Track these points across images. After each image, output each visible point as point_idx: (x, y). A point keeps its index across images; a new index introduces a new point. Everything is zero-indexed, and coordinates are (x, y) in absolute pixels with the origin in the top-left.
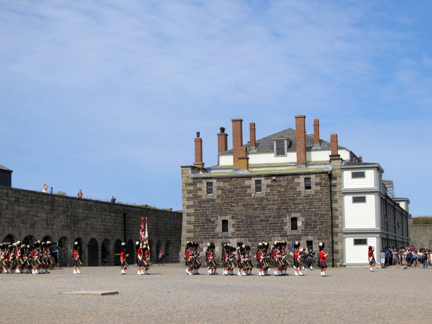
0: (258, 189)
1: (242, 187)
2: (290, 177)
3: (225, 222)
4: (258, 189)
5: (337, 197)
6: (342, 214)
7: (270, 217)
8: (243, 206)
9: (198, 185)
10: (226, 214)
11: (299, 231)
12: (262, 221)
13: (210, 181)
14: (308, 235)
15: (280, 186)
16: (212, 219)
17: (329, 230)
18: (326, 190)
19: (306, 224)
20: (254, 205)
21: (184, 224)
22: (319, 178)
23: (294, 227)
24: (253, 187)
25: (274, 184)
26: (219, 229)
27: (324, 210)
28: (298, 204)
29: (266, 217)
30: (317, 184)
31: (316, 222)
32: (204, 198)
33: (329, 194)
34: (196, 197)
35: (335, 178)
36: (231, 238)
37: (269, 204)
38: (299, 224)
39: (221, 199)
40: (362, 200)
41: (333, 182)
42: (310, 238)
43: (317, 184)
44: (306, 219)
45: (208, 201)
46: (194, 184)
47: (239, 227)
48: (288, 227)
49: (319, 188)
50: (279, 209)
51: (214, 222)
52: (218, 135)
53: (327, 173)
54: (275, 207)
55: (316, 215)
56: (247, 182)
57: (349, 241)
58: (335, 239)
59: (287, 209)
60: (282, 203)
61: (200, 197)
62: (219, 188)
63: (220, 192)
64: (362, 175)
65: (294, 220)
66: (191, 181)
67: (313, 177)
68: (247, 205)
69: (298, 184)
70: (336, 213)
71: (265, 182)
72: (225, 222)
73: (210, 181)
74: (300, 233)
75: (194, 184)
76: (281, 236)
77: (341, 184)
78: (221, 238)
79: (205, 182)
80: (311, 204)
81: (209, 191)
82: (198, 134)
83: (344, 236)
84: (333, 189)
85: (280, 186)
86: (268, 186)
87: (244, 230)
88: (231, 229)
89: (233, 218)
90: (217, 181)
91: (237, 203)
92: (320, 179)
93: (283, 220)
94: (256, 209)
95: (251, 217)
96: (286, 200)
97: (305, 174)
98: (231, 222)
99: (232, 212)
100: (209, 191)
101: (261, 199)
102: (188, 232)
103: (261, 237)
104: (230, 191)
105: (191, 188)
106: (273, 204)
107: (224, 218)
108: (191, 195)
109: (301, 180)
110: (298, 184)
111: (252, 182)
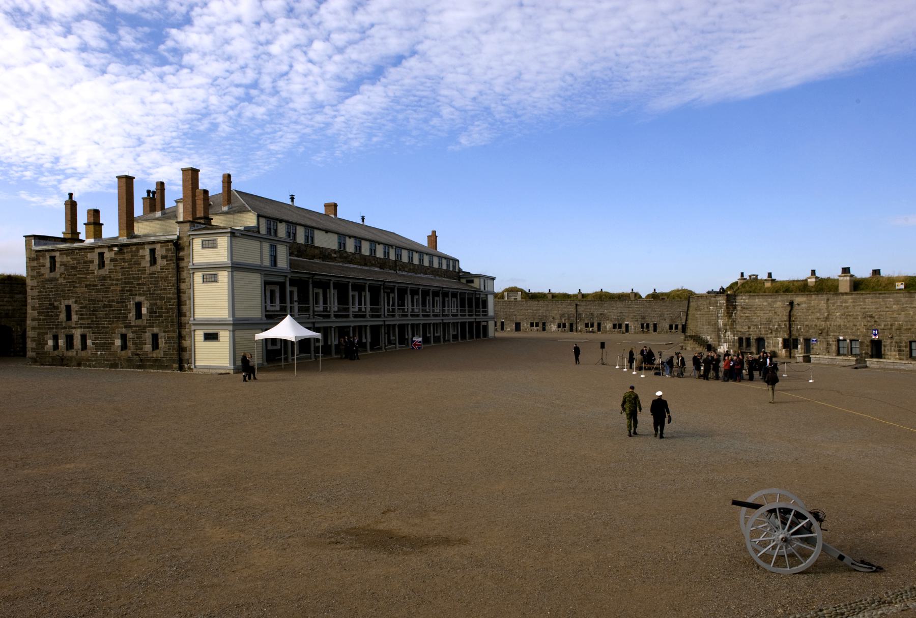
0: (102, 264)
1: (85, 262)
2: (134, 248)
3: (68, 308)
4: (102, 264)
5: (184, 274)
6: (192, 298)
7: (113, 301)
8: (86, 286)
9: (41, 261)
10: (68, 298)
11: (144, 322)
12: (105, 306)
13: (53, 254)
14: (153, 327)
15: (123, 260)
16: (56, 304)
17: (176, 320)
18: (173, 266)
19: (151, 312)
20: (95, 286)
21: (29, 311)
22: (164, 249)
23: (139, 315)
24: (96, 262)
25: (118, 257)
26: (63, 316)
27: (171, 293)
28: (143, 284)
29: (109, 301)
30: (162, 257)
31: (162, 308)
32: (47, 276)
33: (175, 271)
34: (40, 275)
35: (182, 249)
36: (75, 328)
37: (112, 285)
38: (144, 311)
39: (65, 278)
40: (214, 279)
41: (181, 254)
42: (156, 330)
43: (162, 257)
44: (151, 305)
45: (51, 280)
46: (37, 259)
47: (82, 315)
48: (132, 315)
49: (165, 262)
50: (123, 290)
51: (57, 308)
52: (143, 199)
53: (171, 241)
54: (119, 288)
55: (161, 299)
56: (90, 256)
57: (199, 335)
58: (184, 333)
59: (130, 291)
60: (126, 283)
61: (43, 275)
62: (62, 264)
63: (63, 268)
64: (214, 245)
65: (139, 306)
66: (34, 255)
67: (158, 247)
68: (90, 285)
69: (143, 257)
70: (184, 297)
71: (108, 255)
72: (68, 308)
73: (53, 254)
74: (145, 323)
75: (37, 259)
76: (125, 327)
77: (190, 255)
78: (65, 328)
79: (48, 255)
80: (155, 284)
81: (53, 268)
82: (71, 195)
83: (193, 328)
84: (183, 264)
85: (123, 260)
86: (112, 260)
87: (88, 318)
88: (74, 317)
89: (76, 302)
90: (61, 254)
91: (80, 283)
92: (167, 250)
93: (126, 306)
94: (98, 291)
95: (94, 301)
96: (130, 278)
97: (149, 243)
98: (75, 307)
99: (75, 295)
100: (53, 268)
101: (104, 278)
102: (33, 320)
103: (104, 327)
104: (73, 268)
105: (35, 264)
106: (117, 284)
107: (67, 302)
108: (35, 274)
109: (147, 252)
110: (143, 257)
111: (94, 256)
